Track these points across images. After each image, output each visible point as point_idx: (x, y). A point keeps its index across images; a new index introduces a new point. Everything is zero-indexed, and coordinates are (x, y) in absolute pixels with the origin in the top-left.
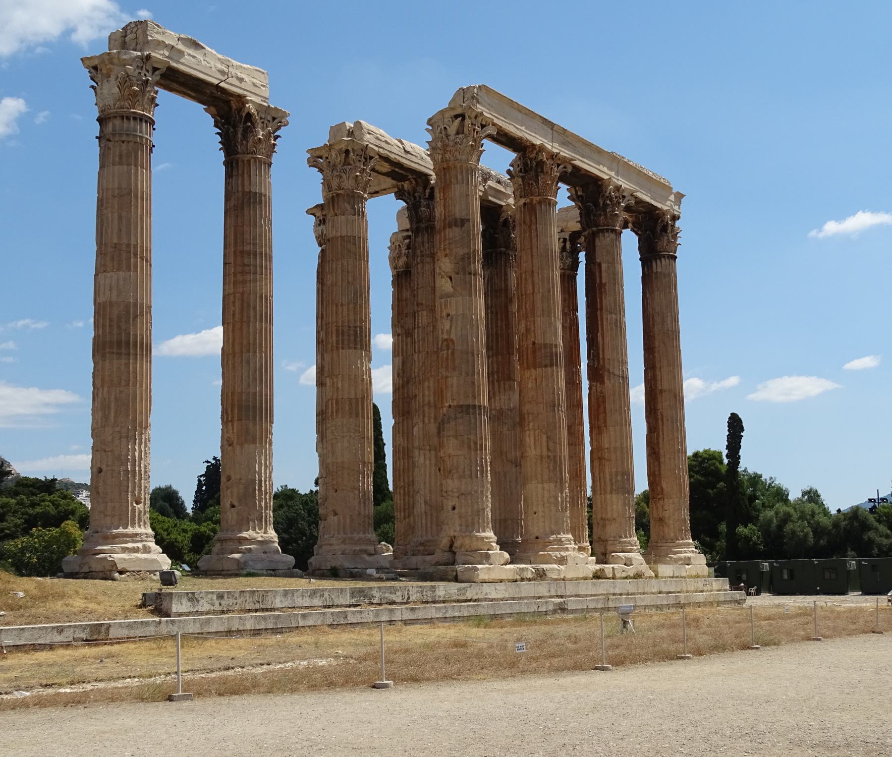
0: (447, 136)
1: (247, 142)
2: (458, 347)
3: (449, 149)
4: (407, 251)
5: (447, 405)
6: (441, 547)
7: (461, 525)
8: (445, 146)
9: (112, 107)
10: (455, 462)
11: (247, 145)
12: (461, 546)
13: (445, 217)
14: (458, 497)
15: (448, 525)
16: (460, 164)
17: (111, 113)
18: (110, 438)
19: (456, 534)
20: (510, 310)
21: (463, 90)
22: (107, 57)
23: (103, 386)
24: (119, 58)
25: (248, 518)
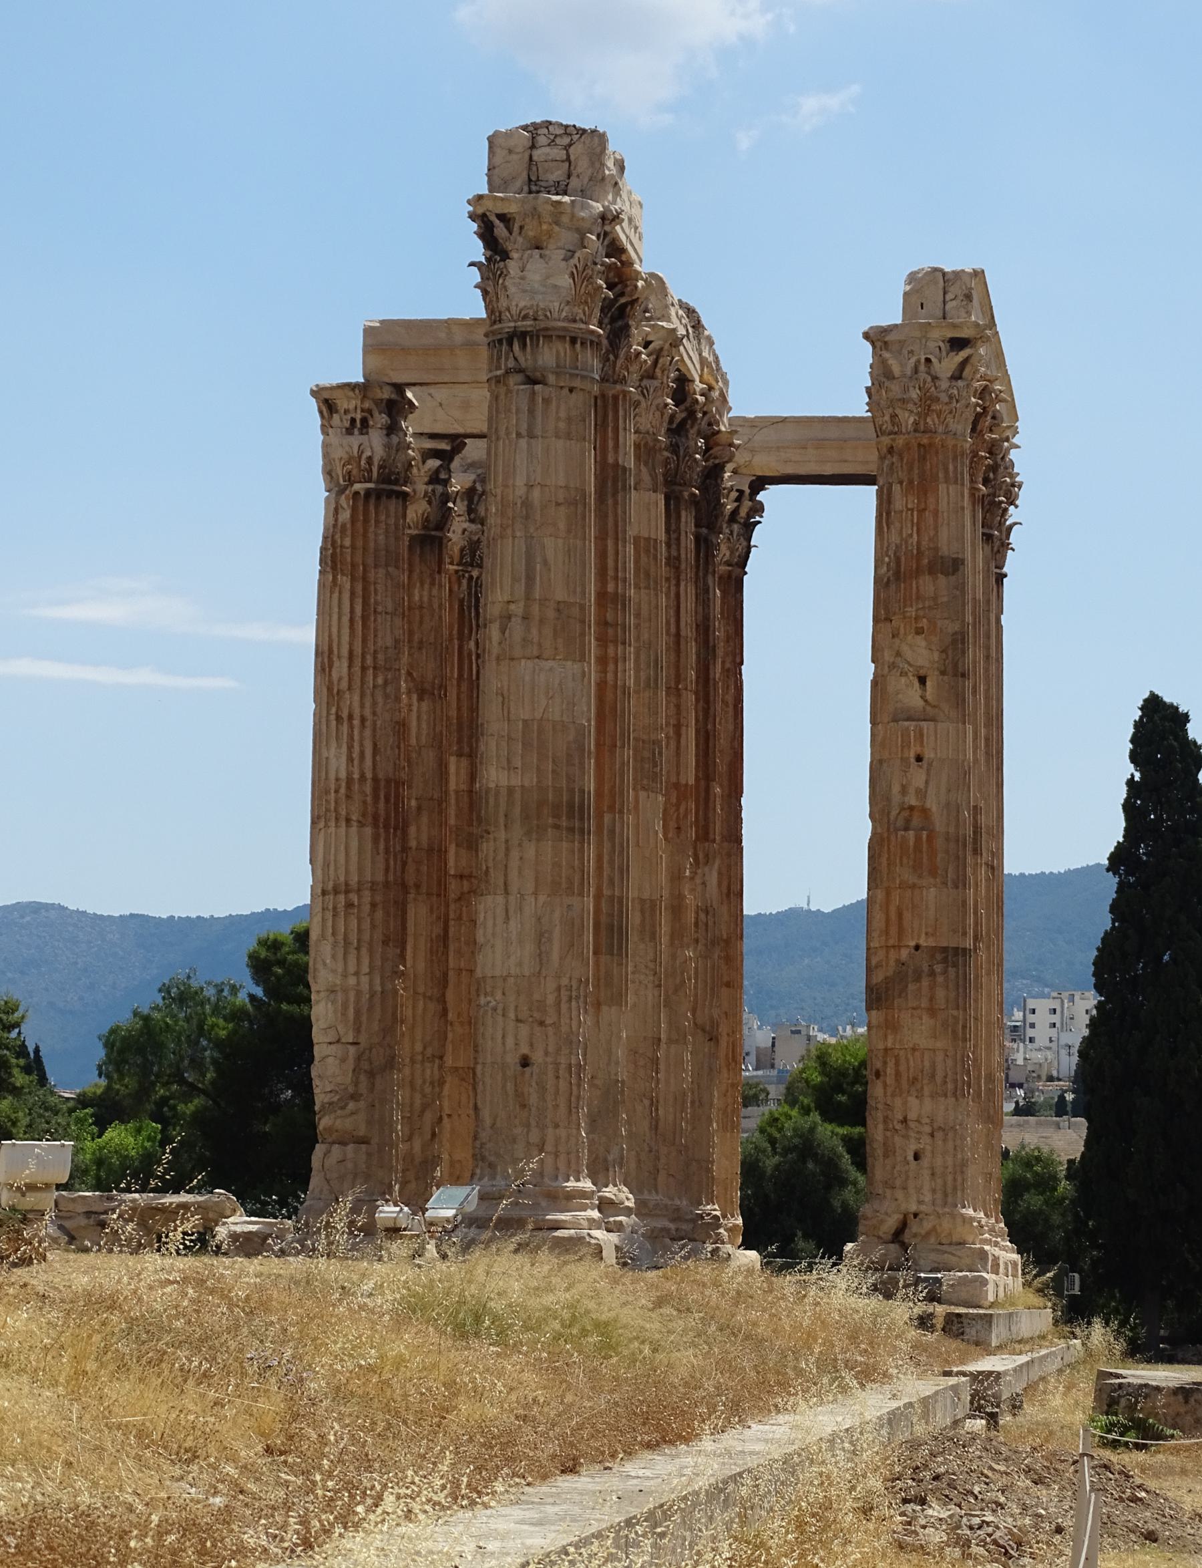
0: (935, 378)
1: (616, 357)
2: (939, 824)
3: (936, 407)
4: (430, 488)
5: (912, 944)
6: (881, 1234)
7: (934, 1191)
8: (927, 402)
9: (556, 315)
10: (927, 1064)
11: (615, 363)
12: (928, 1234)
13: (918, 549)
14: (932, 1135)
15: (905, 1188)
16: (953, 442)
17: (555, 329)
18: (551, 999)
19: (923, 1208)
20: (711, 676)
21: (944, 274)
22: (550, 208)
23: (535, 894)
24: (573, 216)
25: (605, 1160)
